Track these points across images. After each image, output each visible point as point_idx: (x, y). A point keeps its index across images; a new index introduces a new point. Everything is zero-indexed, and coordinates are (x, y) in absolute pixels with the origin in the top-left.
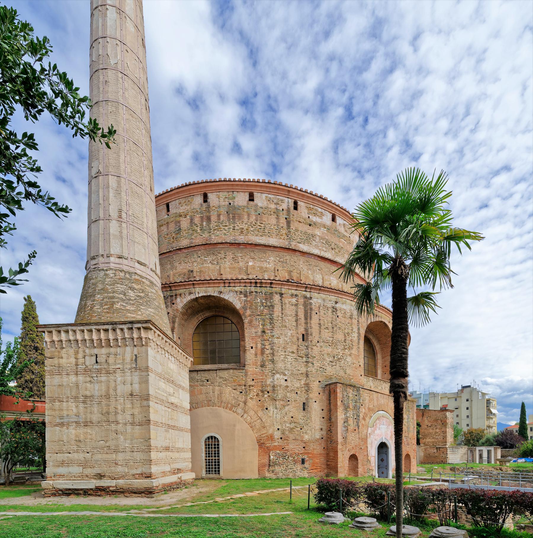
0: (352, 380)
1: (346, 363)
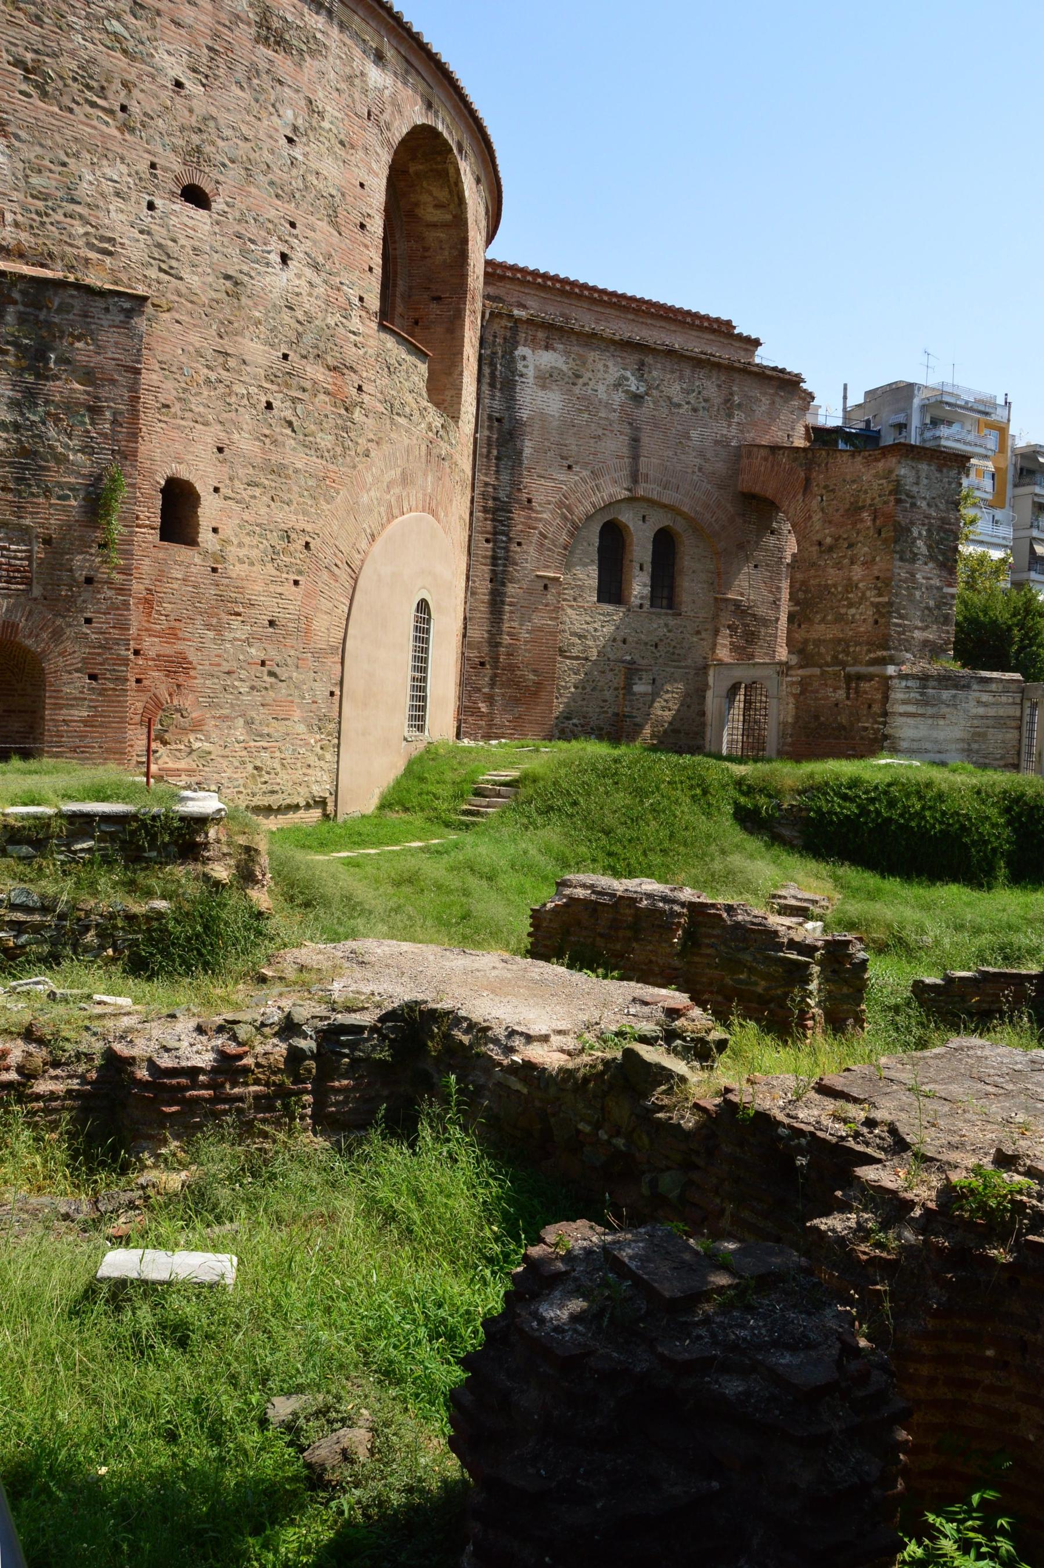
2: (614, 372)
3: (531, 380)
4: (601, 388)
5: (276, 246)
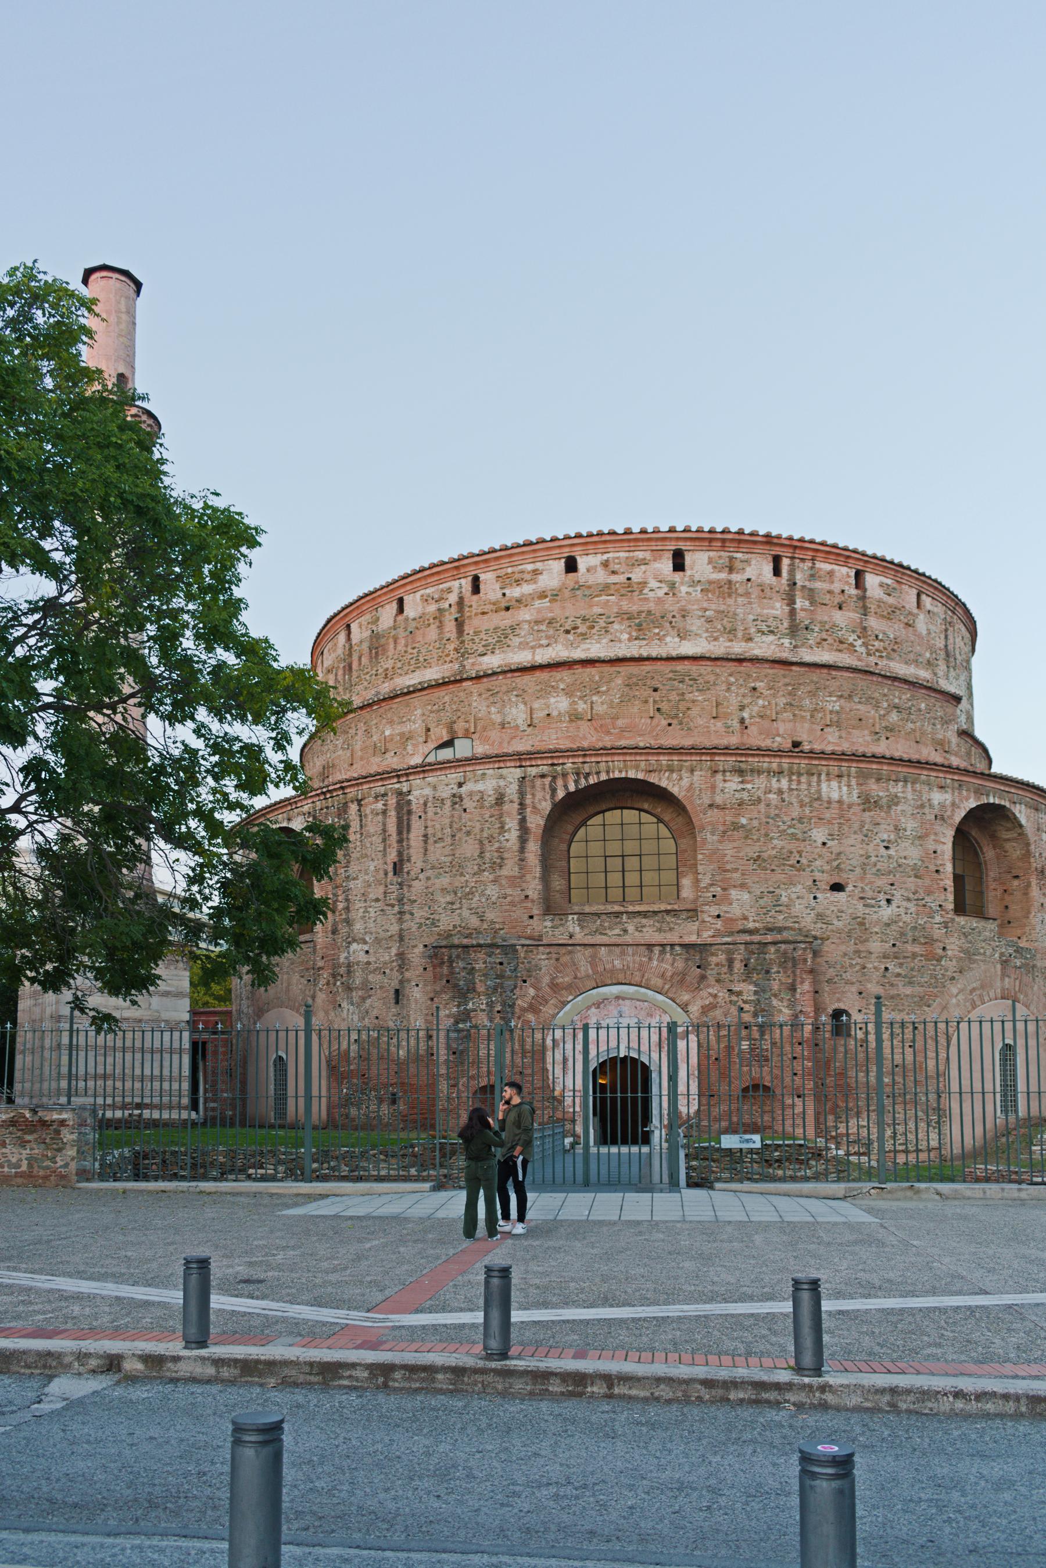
0: (502, 932)
1: (483, 900)
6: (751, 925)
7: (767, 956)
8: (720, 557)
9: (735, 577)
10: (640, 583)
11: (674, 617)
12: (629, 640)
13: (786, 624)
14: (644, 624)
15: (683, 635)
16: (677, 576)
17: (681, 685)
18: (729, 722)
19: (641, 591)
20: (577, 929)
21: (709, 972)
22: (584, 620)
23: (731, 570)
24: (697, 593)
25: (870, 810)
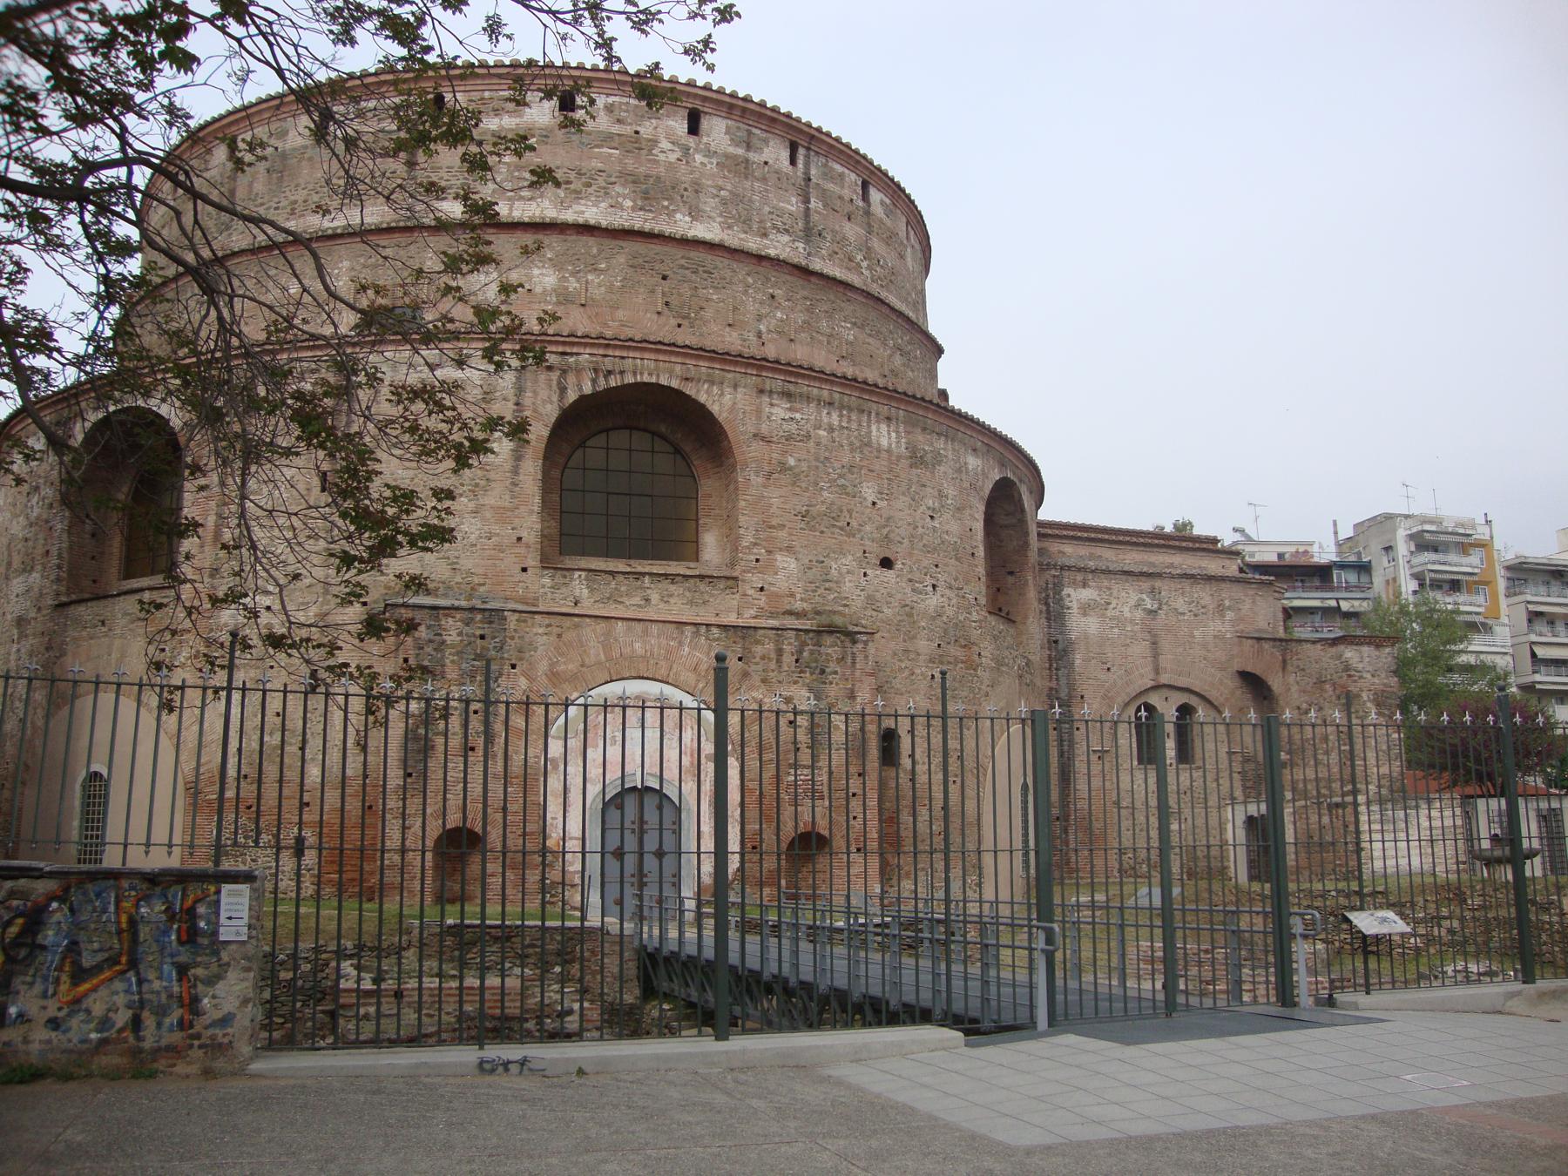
0: (482, 589)
2: (1134, 597)
3: (1075, 610)
4: (1126, 609)
5: (929, 581)
6: (798, 606)
7: (823, 649)
8: (738, 128)
9: (752, 156)
10: (650, 140)
11: (686, 189)
12: (633, 209)
13: (801, 225)
14: (652, 192)
15: (695, 214)
16: (691, 141)
17: (694, 276)
18: (745, 333)
19: (650, 150)
20: (586, 591)
21: (754, 667)
22: (580, 174)
23: (749, 147)
24: (712, 166)
25: (917, 468)
